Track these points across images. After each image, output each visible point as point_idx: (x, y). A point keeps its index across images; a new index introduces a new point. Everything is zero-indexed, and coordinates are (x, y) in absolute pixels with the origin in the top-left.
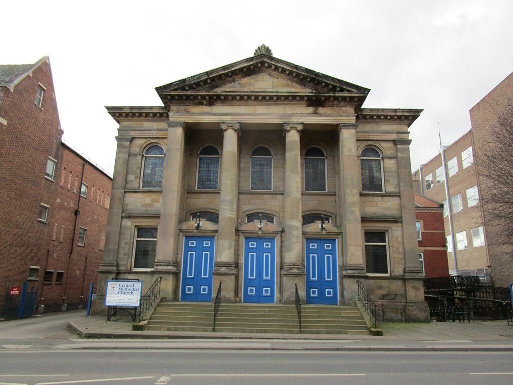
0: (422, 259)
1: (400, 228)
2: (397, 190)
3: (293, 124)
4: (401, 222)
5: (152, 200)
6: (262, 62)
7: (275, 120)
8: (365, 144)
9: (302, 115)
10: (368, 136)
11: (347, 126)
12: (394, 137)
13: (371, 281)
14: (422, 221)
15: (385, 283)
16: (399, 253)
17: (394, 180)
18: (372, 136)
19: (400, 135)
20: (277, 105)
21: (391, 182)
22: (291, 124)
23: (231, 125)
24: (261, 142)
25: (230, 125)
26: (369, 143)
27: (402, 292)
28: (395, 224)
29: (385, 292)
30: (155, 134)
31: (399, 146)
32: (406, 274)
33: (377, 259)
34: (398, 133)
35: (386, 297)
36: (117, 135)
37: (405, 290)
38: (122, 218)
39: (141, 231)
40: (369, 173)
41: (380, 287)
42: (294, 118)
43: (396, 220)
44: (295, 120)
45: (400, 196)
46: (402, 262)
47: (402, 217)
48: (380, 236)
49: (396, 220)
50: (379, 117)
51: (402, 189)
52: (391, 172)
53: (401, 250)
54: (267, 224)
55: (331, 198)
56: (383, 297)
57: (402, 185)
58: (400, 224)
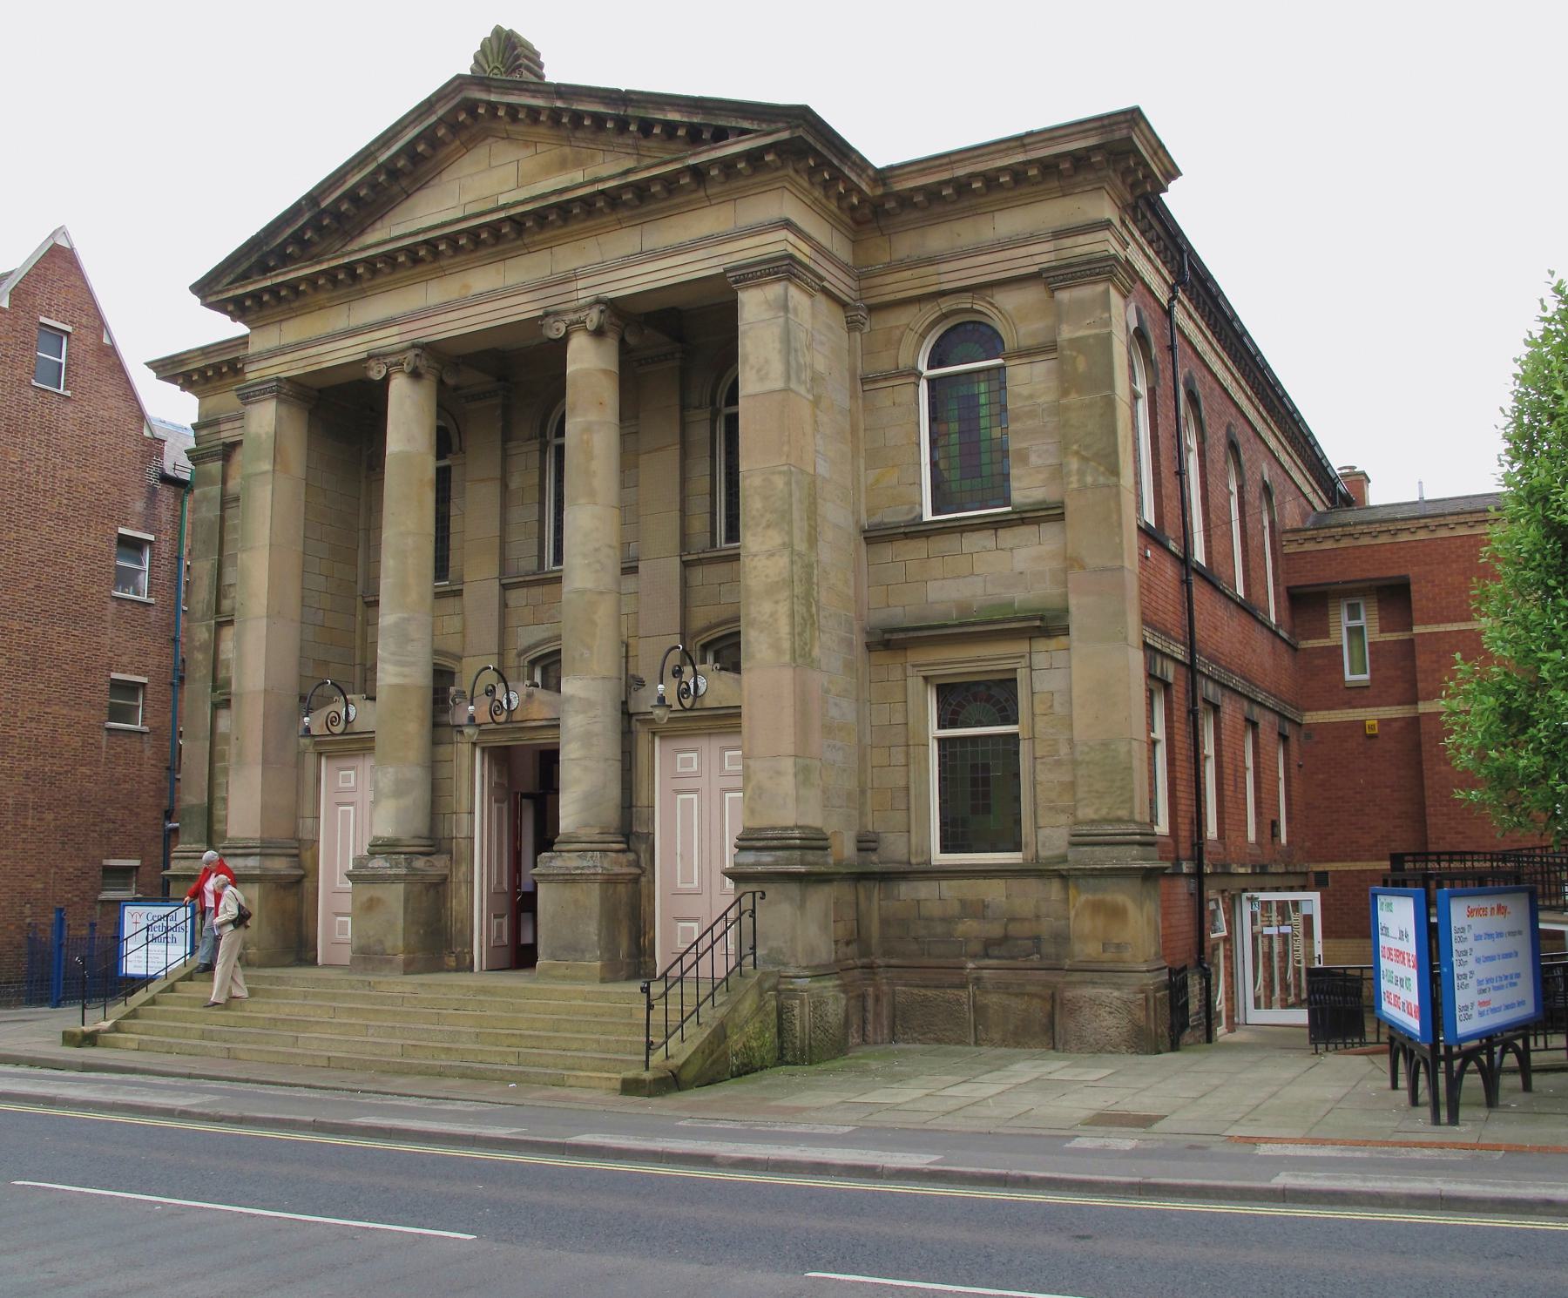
3: (576, 311)
6: (498, 96)
7: (521, 309)
8: (930, 312)
10: (934, 279)
13: (949, 888)
15: (994, 891)
16: (1058, 763)
18: (953, 275)
19: (1068, 242)
20: (528, 249)
21: (1034, 459)
22: (566, 312)
24: (499, 391)
25: (393, 359)
26: (946, 305)
28: (1041, 645)
29: (995, 930)
31: (1064, 296)
33: (981, 795)
34: (1059, 234)
35: (995, 951)
36: (192, 445)
40: (961, 432)
41: (978, 910)
42: (580, 284)
43: (1046, 625)
44: (584, 292)
47: (1067, 611)
48: (997, 696)
49: (1046, 625)
50: (961, 187)
54: (530, 696)
56: (989, 947)
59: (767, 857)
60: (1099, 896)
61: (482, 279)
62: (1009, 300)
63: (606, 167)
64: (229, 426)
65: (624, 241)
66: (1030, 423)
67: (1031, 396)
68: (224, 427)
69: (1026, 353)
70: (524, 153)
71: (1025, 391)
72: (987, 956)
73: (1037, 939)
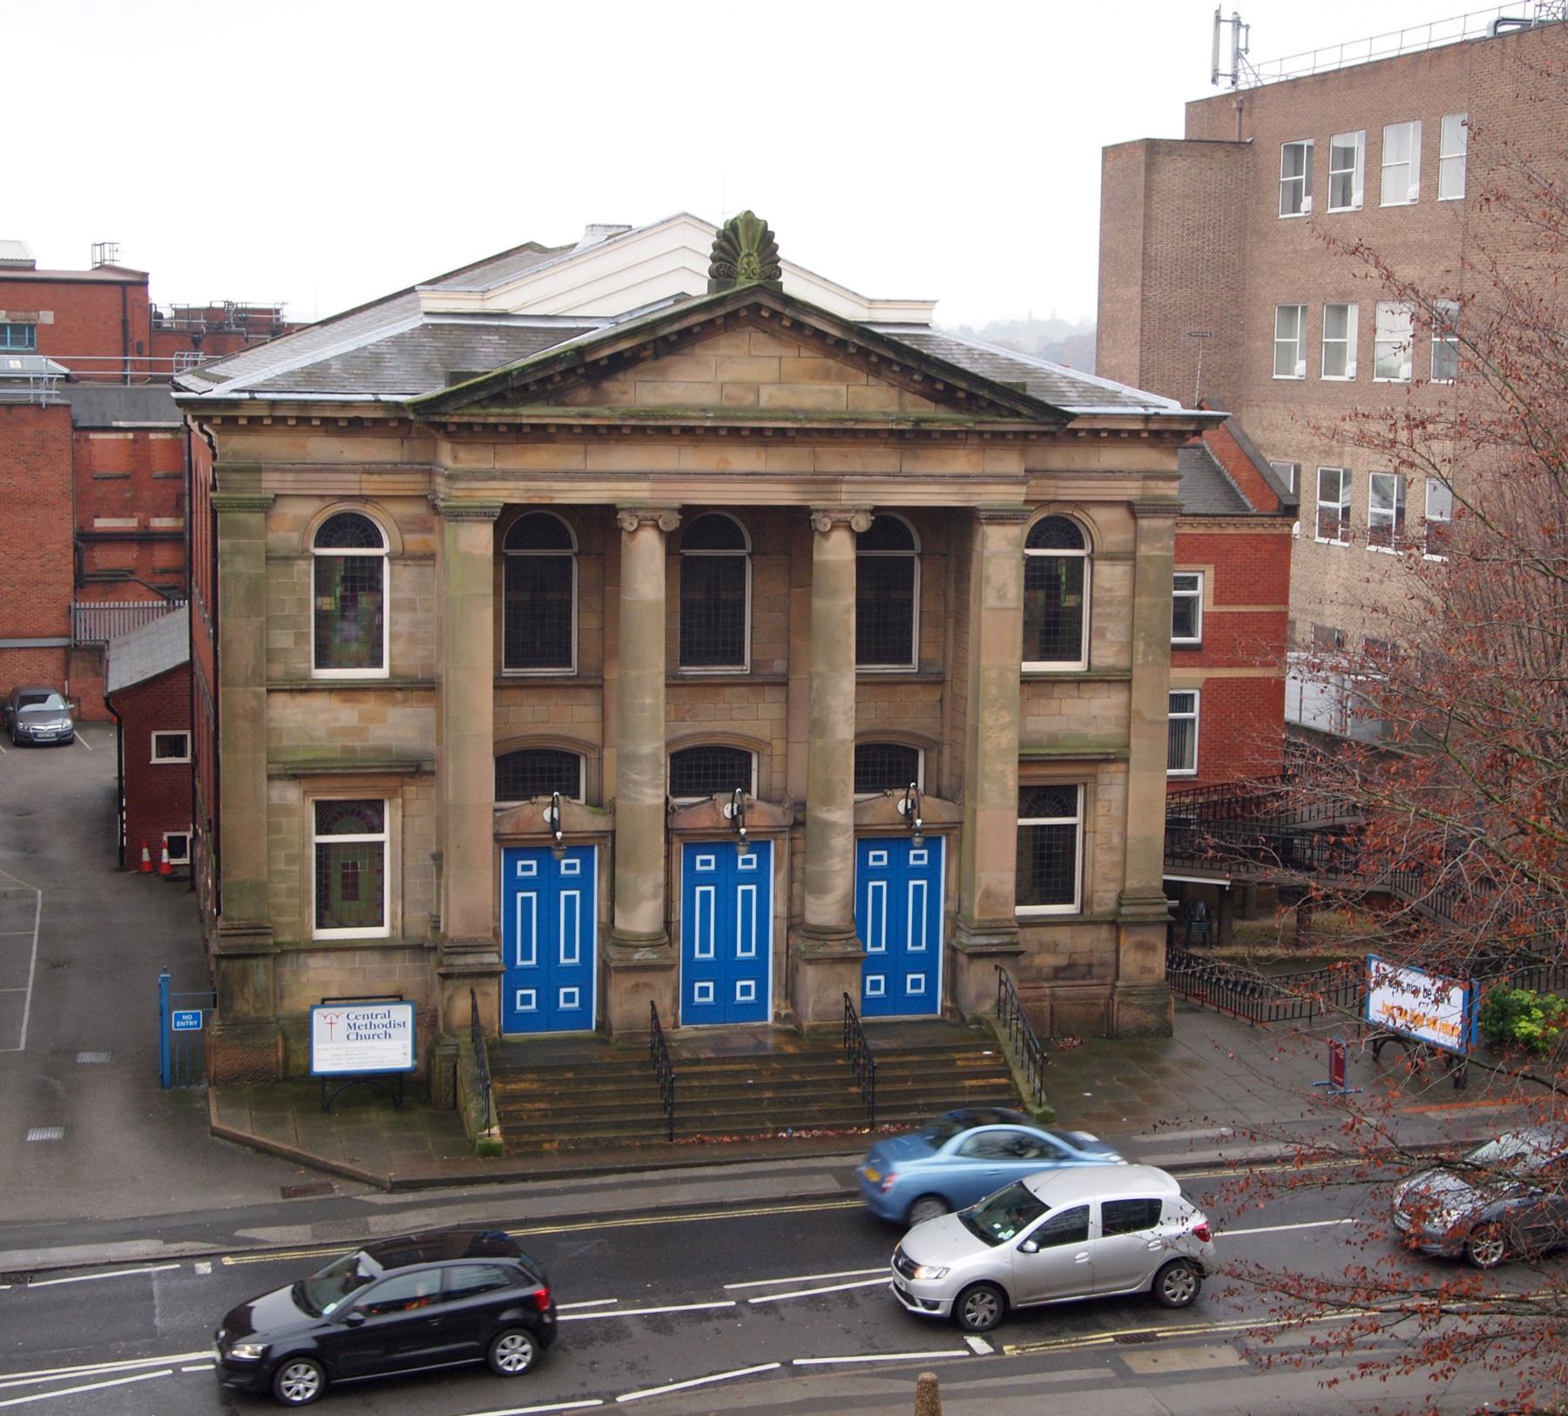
0: (1195, 714)
1: (1120, 778)
2: (1122, 662)
3: (841, 511)
4: (1127, 760)
5: (362, 717)
6: (745, 285)
7: (781, 495)
9: (867, 477)
10: (1052, 490)
11: (1001, 517)
12: (1131, 490)
14: (1210, 571)
15: (1062, 935)
16: (1112, 849)
17: (1116, 632)
19: (1152, 484)
21: (1109, 635)
22: (832, 511)
23: (648, 516)
25: (649, 514)
27: (1111, 958)
29: (1061, 961)
30: (352, 484)
31: (1144, 523)
32: (1124, 910)
33: (1047, 865)
35: (1061, 975)
37: (1117, 951)
38: (270, 777)
39: (329, 816)
41: (1053, 948)
43: (1117, 756)
45: (1129, 682)
46: (1117, 873)
47: (1128, 746)
51: (1139, 659)
52: (1110, 603)
53: (1116, 840)
55: (927, 697)
56: (1058, 973)
57: (1140, 646)
58: (1122, 767)
59: (995, 940)
60: (1139, 938)
61: (743, 459)
62: (1101, 516)
63: (875, 399)
64: (277, 476)
65: (882, 460)
66: (1108, 610)
67: (1109, 590)
68: (265, 476)
69: (1112, 557)
70: (789, 353)
71: (1108, 585)
72: (1056, 978)
73: (1090, 966)
